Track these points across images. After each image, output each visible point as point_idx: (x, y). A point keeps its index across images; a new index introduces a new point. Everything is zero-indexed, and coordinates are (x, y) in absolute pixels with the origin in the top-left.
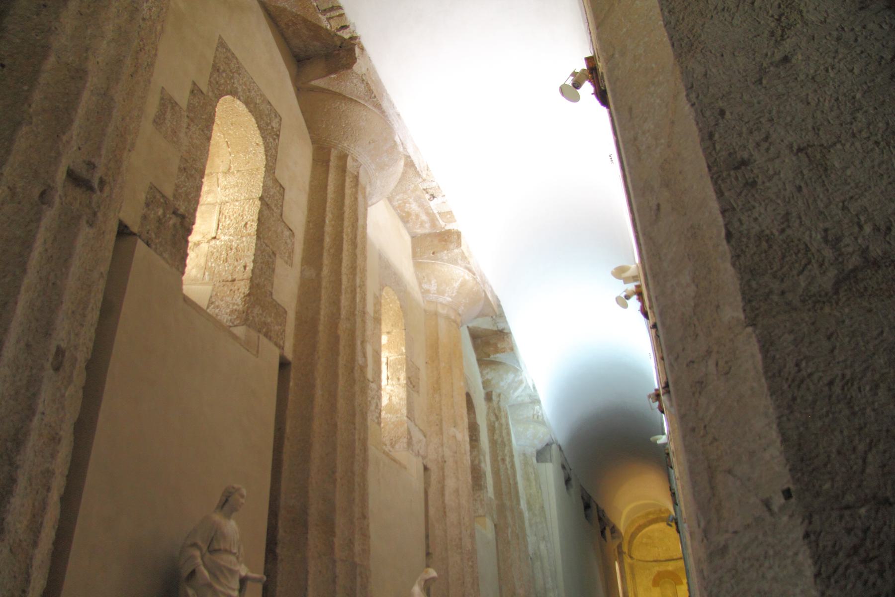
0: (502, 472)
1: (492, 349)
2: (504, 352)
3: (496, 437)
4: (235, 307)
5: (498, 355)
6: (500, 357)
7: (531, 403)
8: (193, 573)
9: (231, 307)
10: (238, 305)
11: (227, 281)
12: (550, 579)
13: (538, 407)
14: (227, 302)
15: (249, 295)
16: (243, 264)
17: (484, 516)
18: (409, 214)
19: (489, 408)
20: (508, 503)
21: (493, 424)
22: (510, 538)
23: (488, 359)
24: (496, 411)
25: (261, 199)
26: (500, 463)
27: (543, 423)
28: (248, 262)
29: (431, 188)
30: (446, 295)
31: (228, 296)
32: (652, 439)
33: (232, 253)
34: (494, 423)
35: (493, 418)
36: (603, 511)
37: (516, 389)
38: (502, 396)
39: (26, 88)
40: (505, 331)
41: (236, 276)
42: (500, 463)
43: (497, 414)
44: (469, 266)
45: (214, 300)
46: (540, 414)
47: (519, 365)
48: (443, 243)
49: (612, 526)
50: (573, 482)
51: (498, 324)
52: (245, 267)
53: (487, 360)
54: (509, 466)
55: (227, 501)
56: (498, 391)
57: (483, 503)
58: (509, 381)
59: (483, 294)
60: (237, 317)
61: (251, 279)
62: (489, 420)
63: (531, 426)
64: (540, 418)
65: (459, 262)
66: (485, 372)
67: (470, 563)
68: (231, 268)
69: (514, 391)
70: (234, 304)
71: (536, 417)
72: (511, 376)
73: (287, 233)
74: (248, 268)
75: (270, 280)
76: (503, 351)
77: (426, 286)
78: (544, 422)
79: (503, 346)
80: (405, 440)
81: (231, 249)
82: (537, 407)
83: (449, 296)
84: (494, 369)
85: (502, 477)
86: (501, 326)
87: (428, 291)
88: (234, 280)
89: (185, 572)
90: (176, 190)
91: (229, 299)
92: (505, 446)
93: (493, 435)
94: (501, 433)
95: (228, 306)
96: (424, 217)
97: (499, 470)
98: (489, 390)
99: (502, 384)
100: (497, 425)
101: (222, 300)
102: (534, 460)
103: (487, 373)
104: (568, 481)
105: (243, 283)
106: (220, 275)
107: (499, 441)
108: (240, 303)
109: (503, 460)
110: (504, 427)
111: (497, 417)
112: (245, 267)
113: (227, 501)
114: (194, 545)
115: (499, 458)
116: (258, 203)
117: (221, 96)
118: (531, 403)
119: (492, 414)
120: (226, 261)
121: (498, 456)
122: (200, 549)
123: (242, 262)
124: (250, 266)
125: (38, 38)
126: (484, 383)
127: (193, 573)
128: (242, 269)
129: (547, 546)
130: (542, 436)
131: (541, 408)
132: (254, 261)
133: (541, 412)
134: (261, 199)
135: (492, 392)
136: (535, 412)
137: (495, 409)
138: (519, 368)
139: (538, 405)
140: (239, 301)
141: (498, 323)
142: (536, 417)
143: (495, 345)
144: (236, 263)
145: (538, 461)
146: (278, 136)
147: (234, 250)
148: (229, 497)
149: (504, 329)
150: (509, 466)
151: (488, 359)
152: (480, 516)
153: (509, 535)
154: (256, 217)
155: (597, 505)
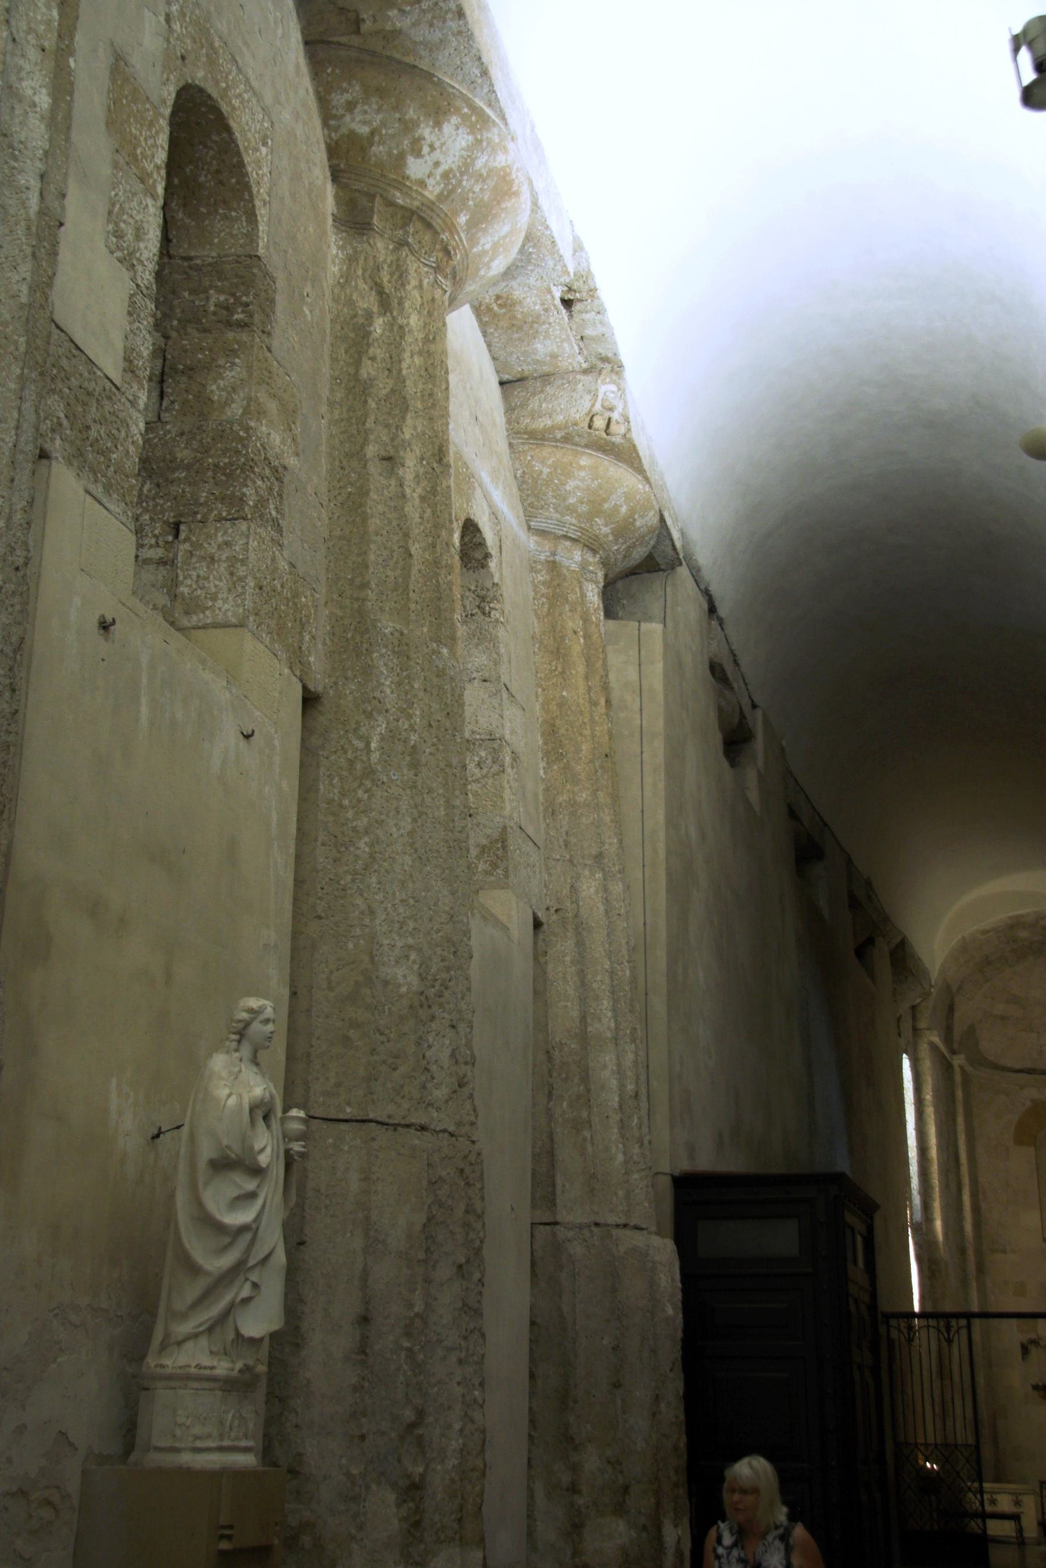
0: (376, 505)
3: (367, 369)
7: (585, 372)
12: (606, 1004)
13: (614, 388)
17: (241, 625)
20: (388, 625)
21: (361, 320)
22: (375, 757)
23: (355, 41)
24: (385, 277)
26: (374, 468)
34: (369, 316)
35: (369, 301)
36: (868, 884)
42: (374, 468)
43: (388, 288)
46: (615, 416)
47: (493, 101)
49: (896, 941)
54: (414, 493)
57: (241, 571)
58: (450, 161)
62: (351, 303)
63: (584, 461)
64: (618, 429)
66: (339, 100)
69: (473, 224)
71: (600, 423)
78: (634, 448)
82: (606, 389)
84: (381, 92)
85: (374, 523)
92: (405, 409)
93: (358, 363)
94: (394, 361)
97: (364, 493)
100: (378, 326)
102: (593, 595)
103: (351, 106)
107: (383, 386)
109: (390, 460)
115: (371, 450)
118: (585, 372)
119: (362, 285)
121: (366, 441)
126: (333, 151)
129: (606, 889)
130: (624, 509)
131: (622, 391)
133: (620, 409)
136: (598, 407)
137: (378, 268)
138: (489, 112)
139: (612, 382)
142: (600, 423)
145: (610, 613)
150: (414, 493)
152: (226, 625)
153: (373, 745)
155: (850, 861)
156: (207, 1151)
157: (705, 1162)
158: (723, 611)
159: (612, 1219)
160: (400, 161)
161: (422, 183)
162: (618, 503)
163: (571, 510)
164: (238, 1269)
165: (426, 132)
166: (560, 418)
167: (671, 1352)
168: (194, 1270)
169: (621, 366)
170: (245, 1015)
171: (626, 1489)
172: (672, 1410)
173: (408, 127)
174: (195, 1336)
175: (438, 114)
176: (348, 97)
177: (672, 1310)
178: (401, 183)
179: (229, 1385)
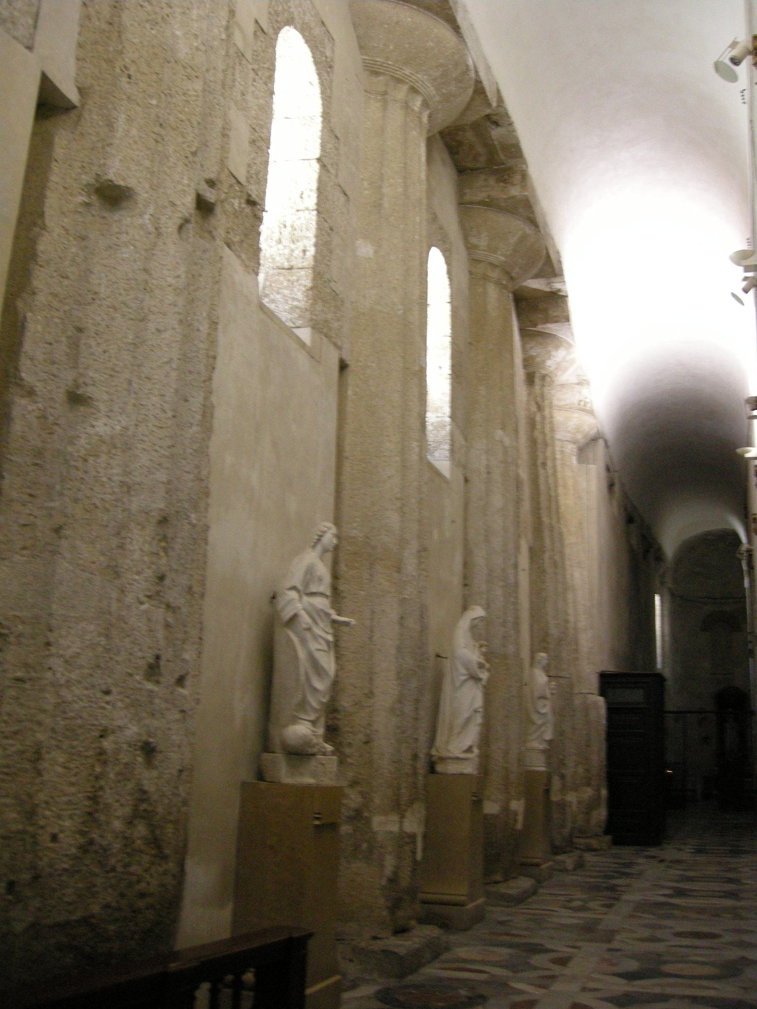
0: (542, 480)
1: (541, 316)
2: (556, 322)
4: (295, 303)
5: (549, 325)
6: (551, 328)
7: (578, 384)
8: (295, 617)
9: (290, 302)
10: (299, 301)
11: (283, 269)
14: (285, 296)
15: (312, 288)
16: (302, 248)
18: (460, 143)
19: (529, 394)
23: (533, 329)
24: (539, 399)
25: (319, 160)
27: (591, 412)
28: (308, 245)
29: (496, 115)
30: (499, 252)
31: (286, 288)
32: (739, 451)
33: (287, 232)
35: (534, 408)
37: (565, 370)
38: (548, 379)
39: (154, 102)
40: (561, 294)
41: (293, 263)
44: (532, 216)
45: (268, 292)
47: (573, 340)
48: (502, 184)
50: (617, 488)
51: (552, 284)
52: (304, 251)
53: (531, 330)
55: (319, 540)
56: (543, 372)
59: (545, 251)
60: (300, 317)
61: (314, 268)
63: (576, 415)
64: (589, 405)
65: (521, 210)
66: (528, 346)
67: (512, 599)
68: (287, 251)
70: (294, 299)
72: (559, 355)
73: (342, 199)
74: (308, 254)
75: (327, 265)
76: (556, 320)
77: (474, 240)
79: (556, 314)
80: (447, 447)
81: (285, 226)
83: (502, 255)
86: (557, 286)
87: (476, 247)
88: (291, 268)
89: (287, 614)
90: (248, 172)
91: (286, 292)
95: (286, 302)
96: (480, 149)
98: (531, 370)
99: (549, 363)
100: (538, 418)
101: (278, 293)
102: (574, 460)
103: (531, 348)
104: (611, 486)
105: (303, 273)
106: (273, 259)
107: (540, 441)
108: (301, 299)
109: (544, 464)
110: (547, 421)
111: (540, 408)
112: (304, 251)
113: (319, 540)
114: (294, 588)
116: (316, 166)
117: (280, 29)
118: (578, 384)
120: (280, 241)
122: (298, 591)
123: (301, 245)
124: (312, 251)
125: (153, 32)
127: (295, 617)
128: (301, 254)
132: (316, 245)
134: (319, 160)
135: (534, 373)
140: (300, 296)
141: (553, 282)
142: (582, 403)
143: (545, 310)
144: (293, 246)
146: (331, 67)
147: (289, 229)
148: (321, 536)
149: (559, 290)
151: (533, 329)
154: (314, 185)
156: (536, 694)
157: (611, 668)
158: (610, 443)
159: (584, 691)
160: (544, 362)
161: (550, 367)
162: (586, 428)
163: (569, 432)
164: (544, 724)
165: (553, 353)
166: (568, 402)
167: (603, 736)
168: (534, 723)
169: (589, 382)
170: (540, 658)
171: (590, 779)
172: (603, 755)
173: (549, 352)
174: (534, 740)
175: (557, 347)
176: (531, 345)
177: (604, 722)
178: (544, 368)
179: (544, 751)
